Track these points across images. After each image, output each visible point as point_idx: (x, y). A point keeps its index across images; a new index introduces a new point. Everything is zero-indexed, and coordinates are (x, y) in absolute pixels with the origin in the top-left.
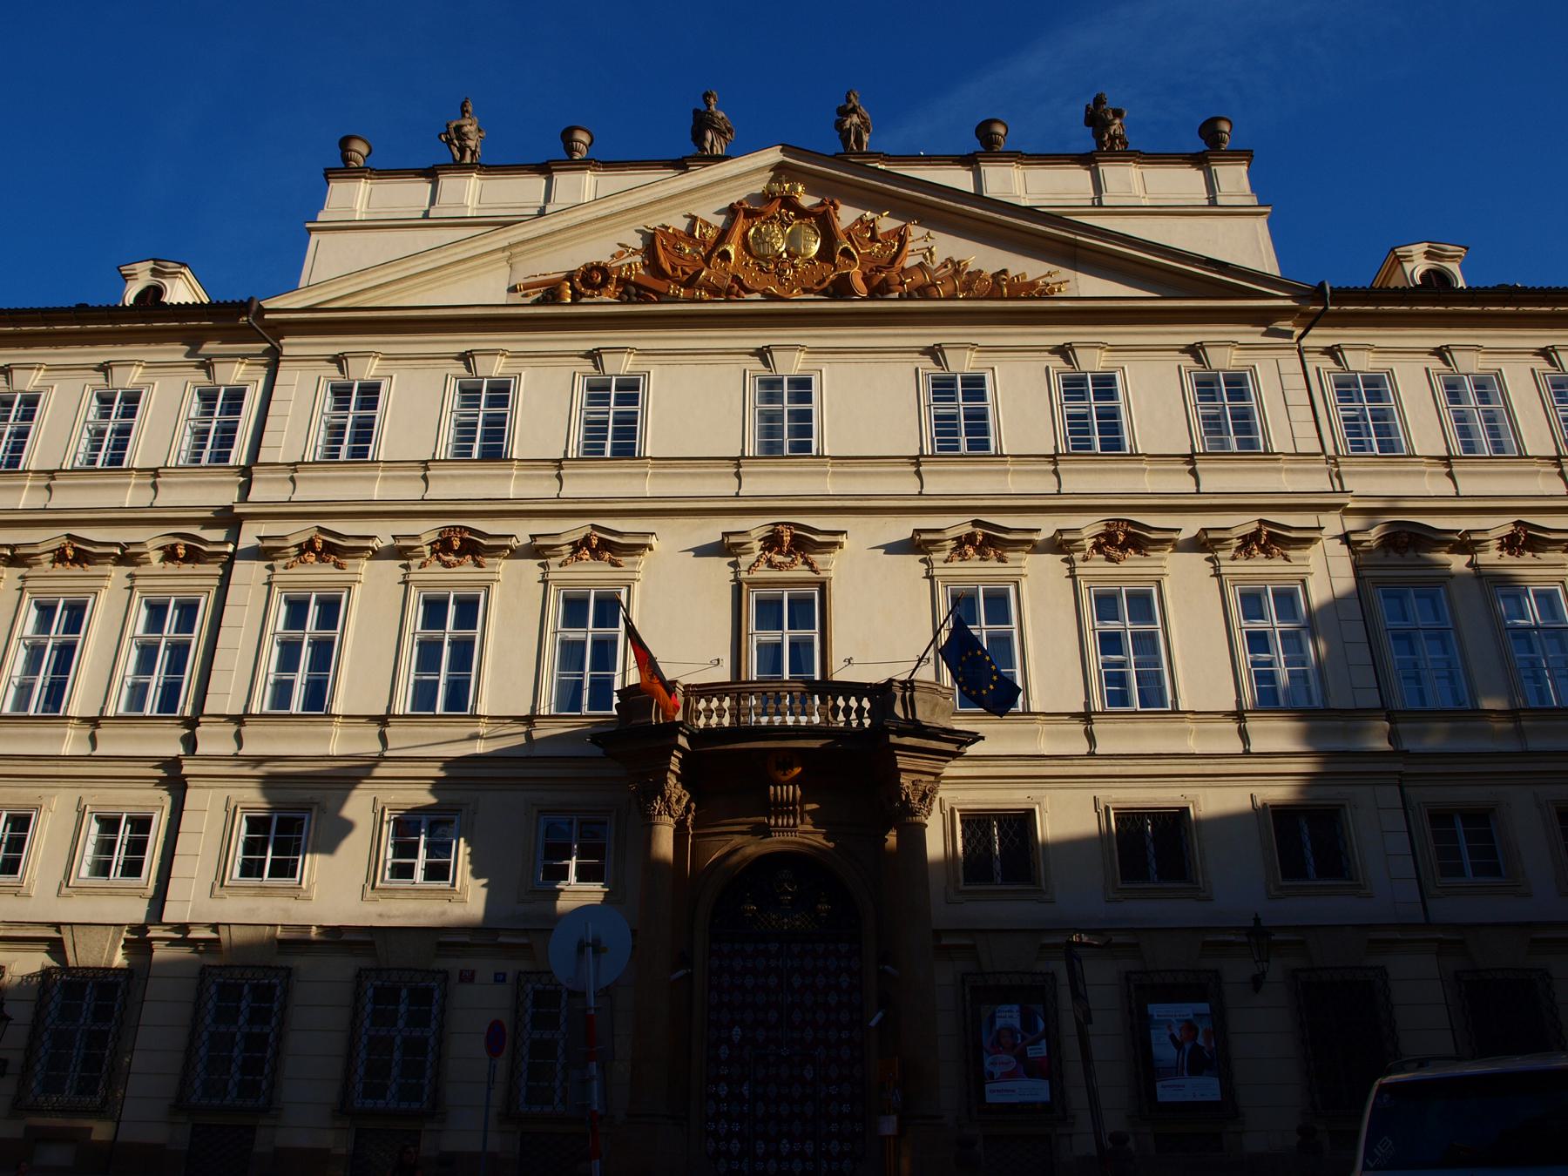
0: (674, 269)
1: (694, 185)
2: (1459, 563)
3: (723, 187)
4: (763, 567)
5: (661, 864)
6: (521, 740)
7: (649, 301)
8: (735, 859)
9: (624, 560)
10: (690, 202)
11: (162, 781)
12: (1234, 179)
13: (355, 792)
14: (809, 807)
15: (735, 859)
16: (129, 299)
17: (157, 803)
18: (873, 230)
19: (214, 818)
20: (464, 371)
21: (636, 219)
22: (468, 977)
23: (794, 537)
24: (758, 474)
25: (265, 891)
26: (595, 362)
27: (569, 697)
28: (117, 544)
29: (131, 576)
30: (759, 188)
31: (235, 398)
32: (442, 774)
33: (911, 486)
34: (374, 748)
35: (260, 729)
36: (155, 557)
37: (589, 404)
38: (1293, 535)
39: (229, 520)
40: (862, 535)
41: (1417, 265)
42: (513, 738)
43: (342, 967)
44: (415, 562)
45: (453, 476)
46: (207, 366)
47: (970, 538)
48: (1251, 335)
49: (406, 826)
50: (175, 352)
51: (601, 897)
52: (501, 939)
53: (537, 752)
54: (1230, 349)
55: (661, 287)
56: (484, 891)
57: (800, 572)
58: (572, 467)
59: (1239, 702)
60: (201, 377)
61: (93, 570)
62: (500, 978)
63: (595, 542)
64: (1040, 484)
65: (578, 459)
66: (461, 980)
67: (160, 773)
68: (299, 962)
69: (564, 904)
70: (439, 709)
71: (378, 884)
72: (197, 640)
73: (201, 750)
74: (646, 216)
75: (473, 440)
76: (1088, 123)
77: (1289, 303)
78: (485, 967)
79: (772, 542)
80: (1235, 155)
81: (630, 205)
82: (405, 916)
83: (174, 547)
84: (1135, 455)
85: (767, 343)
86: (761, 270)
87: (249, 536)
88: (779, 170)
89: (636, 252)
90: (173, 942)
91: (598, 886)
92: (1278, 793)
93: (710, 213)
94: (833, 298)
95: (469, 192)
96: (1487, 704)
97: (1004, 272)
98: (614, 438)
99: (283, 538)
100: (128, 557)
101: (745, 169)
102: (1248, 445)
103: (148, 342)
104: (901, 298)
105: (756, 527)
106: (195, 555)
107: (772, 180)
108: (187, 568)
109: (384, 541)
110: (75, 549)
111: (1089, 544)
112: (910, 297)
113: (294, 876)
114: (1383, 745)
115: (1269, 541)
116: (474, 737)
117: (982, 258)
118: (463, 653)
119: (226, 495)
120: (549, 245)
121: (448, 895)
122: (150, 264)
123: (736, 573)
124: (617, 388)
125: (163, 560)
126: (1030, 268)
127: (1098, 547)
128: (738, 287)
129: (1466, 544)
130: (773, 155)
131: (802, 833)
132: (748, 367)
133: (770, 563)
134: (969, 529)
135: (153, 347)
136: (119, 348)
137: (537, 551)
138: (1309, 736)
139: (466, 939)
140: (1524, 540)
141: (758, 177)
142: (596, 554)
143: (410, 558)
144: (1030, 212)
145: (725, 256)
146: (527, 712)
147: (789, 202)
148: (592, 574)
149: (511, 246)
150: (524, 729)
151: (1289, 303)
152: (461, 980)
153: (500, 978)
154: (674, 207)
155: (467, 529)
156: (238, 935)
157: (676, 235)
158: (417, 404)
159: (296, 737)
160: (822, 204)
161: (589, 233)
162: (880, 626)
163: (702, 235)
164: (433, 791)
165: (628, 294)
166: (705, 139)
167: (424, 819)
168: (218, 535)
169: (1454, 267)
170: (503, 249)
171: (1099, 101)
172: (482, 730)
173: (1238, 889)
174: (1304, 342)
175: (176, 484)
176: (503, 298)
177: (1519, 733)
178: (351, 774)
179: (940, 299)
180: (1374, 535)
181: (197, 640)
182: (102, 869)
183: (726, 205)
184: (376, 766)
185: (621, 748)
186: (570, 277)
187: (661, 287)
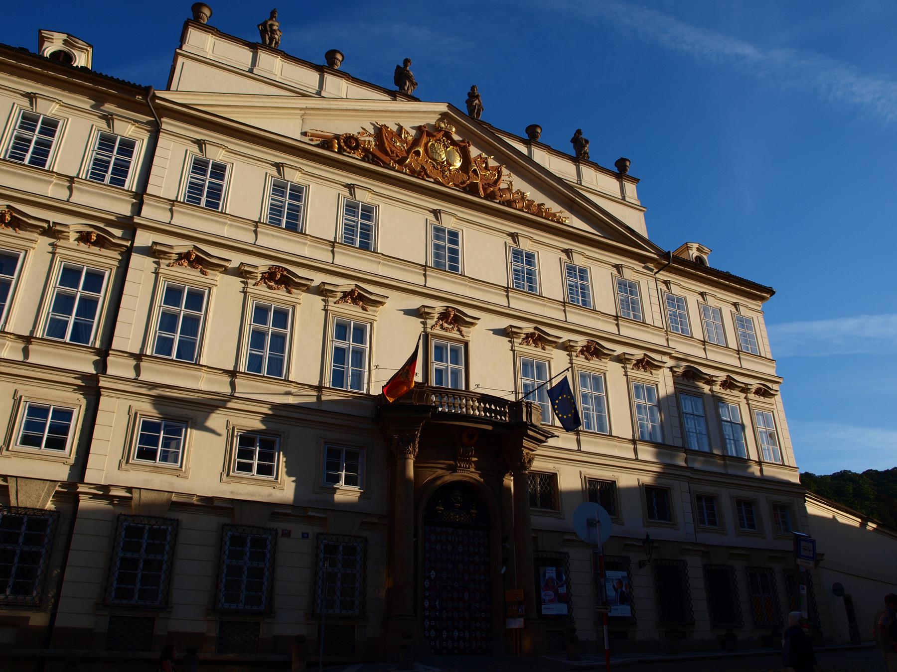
1: (404, 109)
2: (706, 389)
3: (416, 115)
4: (438, 328)
5: (409, 480)
6: (314, 399)
7: (380, 166)
8: (439, 482)
9: (369, 308)
10: (399, 117)
11: (79, 388)
12: (631, 189)
13: (213, 415)
14: (475, 459)
15: (439, 482)
16: (47, 53)
17: (77, 403)
18: (487, 164)
19: (116, 420)
20: (276, 174)
21: (372, 117)
22: (287, 534)
23: (455, 315)
24: (436, 277)
25: (157, 470)
26: (350, 191)
27: (338, 378)
28: (48, 222)
29: (51, 244)
30: (433, 122)
31: (127, 147)
32: (270, 412)
33: (420, 280)
34: (227, 390)
35: (153, 365)
36: (73, 236)
37: (21, 127)
38: (656, 363)
39: (129, 226)
40: (396, 302)
41: (694, 253)
42: (310, 398)
43: (211, 522)
44: (574, 354)
45: (273, 235)
46: (108, 118)
47: (532, 335)
48: (639, 266)
49: (247, 440)
50: (86, 103)
51: (359, 494)
52: (310, 513)
53: (324, 408)
54: (633, 271)
55: (377, 157)
56: (294, 484)
57: (455, 334)
58: (339, 248)
59: (633, 436)
60: (103, 124)
61: (23, 234)
62: (305, 536)
63: (193, 257)
64: (322, 255)
65: (183, 203)
66: (283, 535)
67: (79, 382)
68: (183, 517)
69: (339, 497)
70: (67, 339)
71: (231, 473)
72: (103, 297)
73: (110, 371)
74: (376, 117)
75: (27, 151)
76: (572, 141)
77: (655, 256)
78: (297, 529)
79: (444, 316)
80: (635, 180)
82: (247, 494)
83: (89, 234)
84: (594, 310)
85: (353, 182)
86: (434, 166)
87: (143, 239)
88: (444, 115)
89: (370, 135)
90: (95, 496)
91: (356, 488)
92: (647, 479)
93: (409, 125)
94: (465, 192)
95: (272, 64)
96: (716, 452)
97: (543, 204)
98: (33, 153)
99: (171, 247)
100: (52, 232)
101: (429, 110)
102: (454, 269)
103: (64, 89)
104: (499, 203)
105: (439, 306)
106: (102, 242)
107: (439, 120)
108: (95, 250)
109: (234, 264)
110: (12, 216)
111: (579, 349)
112: (503, 204)
113: (176, 462)
114: (683, 464)
115: (646, 364)
116: (288, 393)
117: (532, 193)
118: (279, 342)
119: (125, 209)
121: (274, 485)
122: (65, 36)
123: (424, 328)
124: (42, 123)
125: (78, 240)
127: (582, 352)
128: (422, 173)
129: (710, 381)
130: (443, 108)
131: (470, 473)
132: (269, 172)
133: (442, 327)
134: (532, 330)
135: (66, 93)
136: (39, 86)
137: (322, 291)
138: (658, 455)
139: (289, 511)
140: (729, 384)
142: (354, 301)
143: (248, 278)
144: (559, 180)
146: (27, 334)
147: (448, 135)
148: (351, 311)
149: (306, 108)
150: (315, 393)
151: (655, 256)
152: (283, 535)
153: (305, 536)
154: (391, 117)
155: (286, 269)
156: (146, 496)
157: (392, 132)
158: (248, 185)
159: (597, 444)
160: (463, 141)
161: (347, 116)
162: (492, 371)
163: (405, 138)
164: (263, 421)
165: (368, 158)
166: (405, 84)
167: (258, 437)
168: (118, 232)
169: (705, 257)
170: (301, 109)
171: (579, 132)
172: (293, 390)
173: (633, 520)
175: (87, 191)
176: (298, 136)
177: (725, 466)
178: (213, 404)
179: (516, 209)
180: (680, 370)
181: (103, 297)
182: (27, 440)
183: (417, 125)
184: (229, 401)
185: (414, 418)
186: (337, 137)
187: (377, 157)
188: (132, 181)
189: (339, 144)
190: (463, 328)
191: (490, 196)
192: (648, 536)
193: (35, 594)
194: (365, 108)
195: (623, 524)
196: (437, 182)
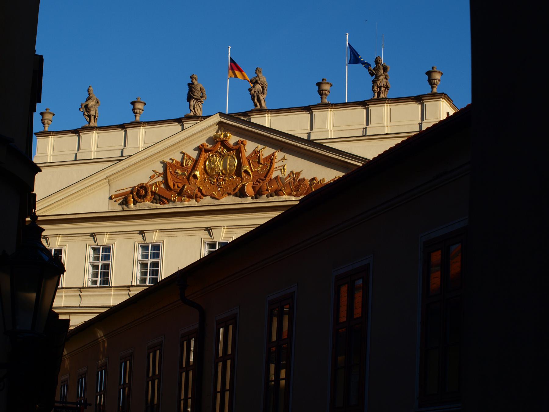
0: (174, 185)
45: (90, 295)
81: (155, 152)
120: (124, 174)
130: (217, 118)
141: (211, 129)
145: (195, 177)
147: (224, 143)
154: (175, 149)
163: (187, 164)
170: (105, 179)
189: (133, 198)
194: (149, 155)
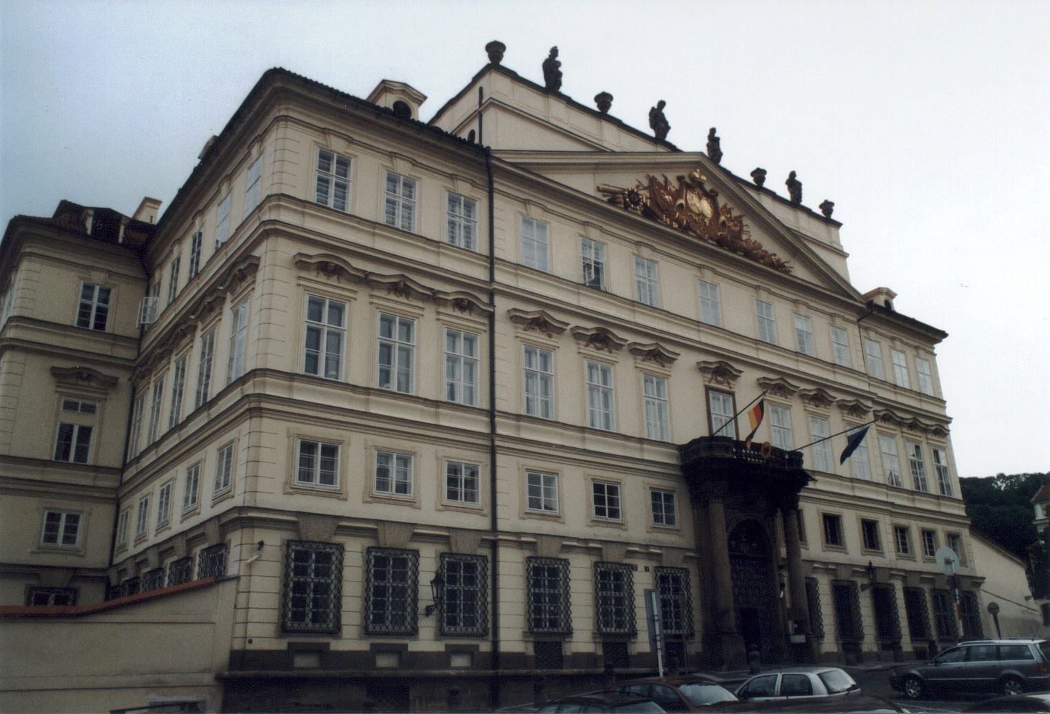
52: (652, 550)
62: (647, 569)
126: (782, 255)
153: (647, 569)
174: (861, 323)
188: (481, 246)
189: (624, 199)
190: (731, 382)
191: (734, 250)
192: (870, 563)
193: (478, 625)
195: (847, 554)
196: (700, 238)
